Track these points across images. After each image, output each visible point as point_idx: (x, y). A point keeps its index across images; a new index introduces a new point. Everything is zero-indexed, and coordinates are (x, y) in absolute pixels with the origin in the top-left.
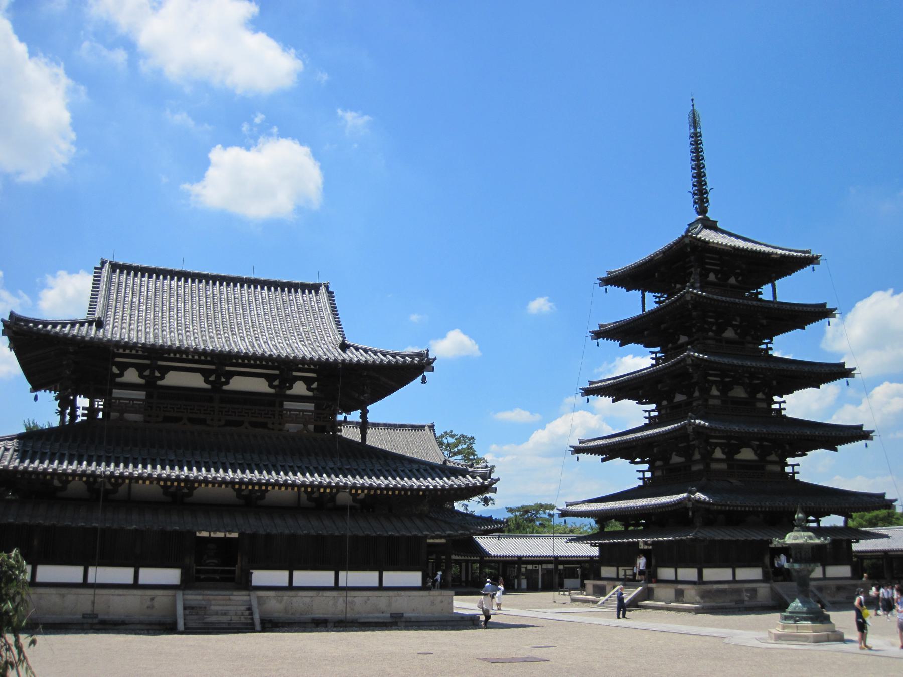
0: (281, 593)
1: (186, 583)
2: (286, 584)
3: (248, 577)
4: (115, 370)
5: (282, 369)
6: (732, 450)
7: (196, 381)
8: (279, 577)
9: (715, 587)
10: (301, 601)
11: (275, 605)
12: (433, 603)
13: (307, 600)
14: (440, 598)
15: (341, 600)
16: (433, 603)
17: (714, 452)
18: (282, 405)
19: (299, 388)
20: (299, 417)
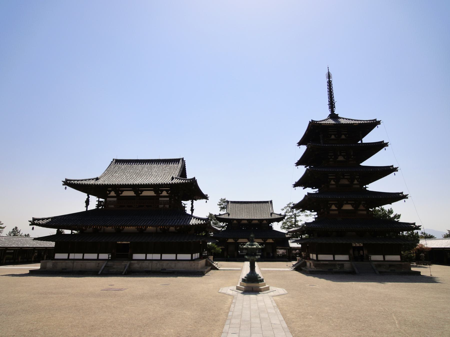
0: (138, 262)
1: (113, 259)
2: (160, 258)
3: (132, 256)
4: (108, 192)
5: (157, 188)
6: (340, 206)
7: (132, 194)
8: (142, 256)
9: (322, 262)
10: (165, 264)
11: (136, 266)
12: (191, 266)
13: (147, 264)
14: (193, 264)
15: (151, 264)
16: (191, 266)
17: (331, 207)
18: (159, 199)
19: (164, 193)
20: (165, 203)
